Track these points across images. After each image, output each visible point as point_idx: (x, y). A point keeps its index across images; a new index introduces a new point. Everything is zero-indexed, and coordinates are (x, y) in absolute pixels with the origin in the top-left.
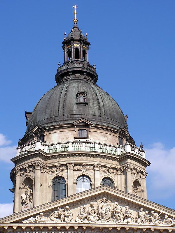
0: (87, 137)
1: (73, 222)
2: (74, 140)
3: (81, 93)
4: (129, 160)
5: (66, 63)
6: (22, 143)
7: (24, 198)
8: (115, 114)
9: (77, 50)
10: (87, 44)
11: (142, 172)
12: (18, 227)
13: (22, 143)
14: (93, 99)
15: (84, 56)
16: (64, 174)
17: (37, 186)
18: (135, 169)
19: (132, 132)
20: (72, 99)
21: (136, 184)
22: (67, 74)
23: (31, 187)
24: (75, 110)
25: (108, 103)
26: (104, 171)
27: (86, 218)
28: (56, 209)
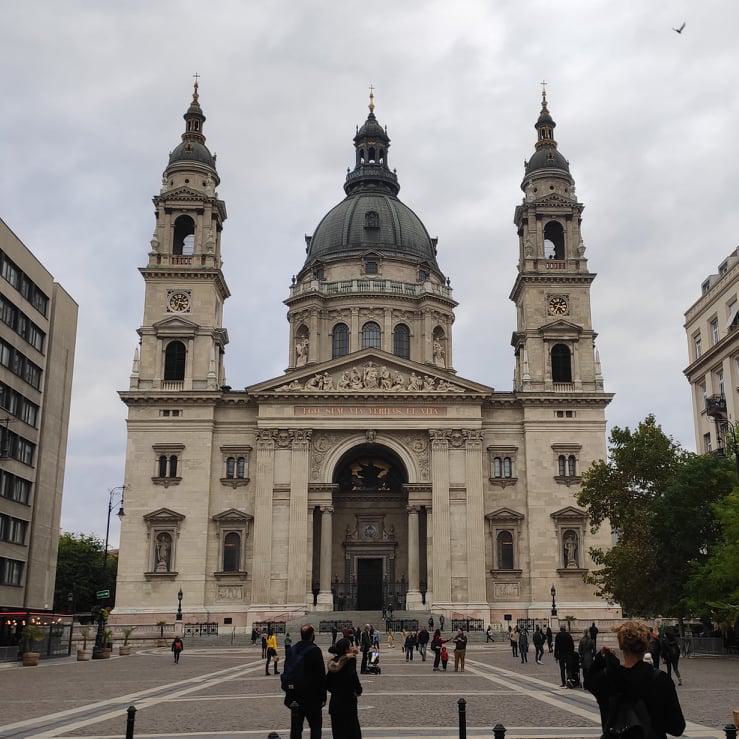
0: (376, 272)
1: (333, 390)
2: (360, 277)
3: (370, 213)
5: (357, 169)
10: (385, 140)
12: (269, 396)
16: (346, 321)
17: (313, 335)
19: (443, 263)
20: (361, 222)
23: (307, 337)
24: (363, 237)
26: (397, 316)
27: (348, 385)
28: (313, 376)
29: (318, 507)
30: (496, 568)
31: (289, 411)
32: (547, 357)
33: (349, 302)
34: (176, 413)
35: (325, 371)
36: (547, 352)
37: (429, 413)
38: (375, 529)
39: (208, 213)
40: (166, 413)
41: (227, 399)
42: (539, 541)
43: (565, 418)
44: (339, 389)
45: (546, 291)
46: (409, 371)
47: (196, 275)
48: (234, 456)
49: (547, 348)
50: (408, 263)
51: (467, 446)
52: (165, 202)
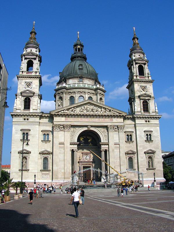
1: (77, 112)
4: (98, 90)
5: (75, 53)
6: (59, 83)
7: (59, 104)
8: (93, 73)
9: (79, 48)
10: (83, 46)
11: (103, 95)
13: (59, 83)
14: (85, 67)
15: (81, 51)
16: (74, 95)
17: (64, 100)
18: (100, 93)
20: (77, 67)
21: (101, 99)
22: (75, 57)
25: (91, 69)
28: (71, 108)
29: (73, 150)
30: (128, 168)
31: (63, 119)
32: (142, 104)
33: (74, 90)
34: (28, 119)
35: (75, 107)
36: (142, 103)
37: (107, 120)
38: (88, 158)
39: (37, 59)
40: (25, 119)
41: (43, 115)
42: (143, 159)
43: (148, 123)
44: (80, 112)
45: (140, 84)
46: (101, 107)
47: (34, 77)
48: (45, 133)
49: (142, 101)
50: (92, 80)
51: (120, 131)
52: (24, 56)
